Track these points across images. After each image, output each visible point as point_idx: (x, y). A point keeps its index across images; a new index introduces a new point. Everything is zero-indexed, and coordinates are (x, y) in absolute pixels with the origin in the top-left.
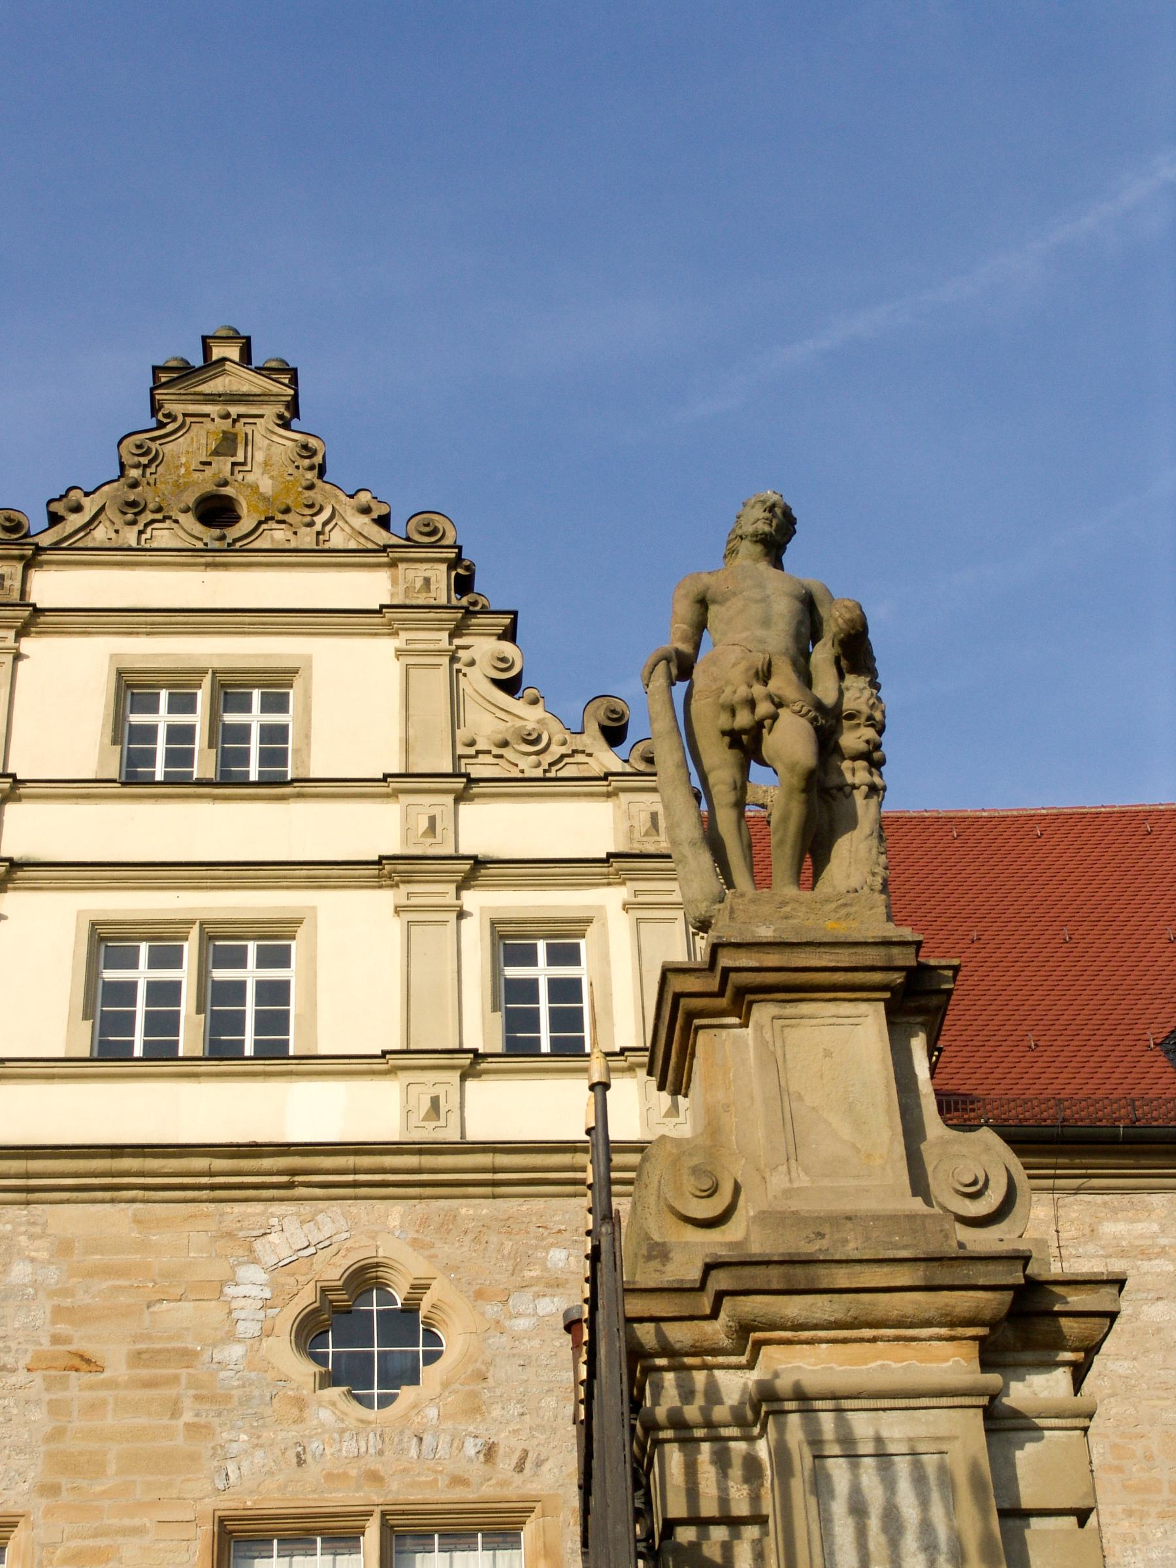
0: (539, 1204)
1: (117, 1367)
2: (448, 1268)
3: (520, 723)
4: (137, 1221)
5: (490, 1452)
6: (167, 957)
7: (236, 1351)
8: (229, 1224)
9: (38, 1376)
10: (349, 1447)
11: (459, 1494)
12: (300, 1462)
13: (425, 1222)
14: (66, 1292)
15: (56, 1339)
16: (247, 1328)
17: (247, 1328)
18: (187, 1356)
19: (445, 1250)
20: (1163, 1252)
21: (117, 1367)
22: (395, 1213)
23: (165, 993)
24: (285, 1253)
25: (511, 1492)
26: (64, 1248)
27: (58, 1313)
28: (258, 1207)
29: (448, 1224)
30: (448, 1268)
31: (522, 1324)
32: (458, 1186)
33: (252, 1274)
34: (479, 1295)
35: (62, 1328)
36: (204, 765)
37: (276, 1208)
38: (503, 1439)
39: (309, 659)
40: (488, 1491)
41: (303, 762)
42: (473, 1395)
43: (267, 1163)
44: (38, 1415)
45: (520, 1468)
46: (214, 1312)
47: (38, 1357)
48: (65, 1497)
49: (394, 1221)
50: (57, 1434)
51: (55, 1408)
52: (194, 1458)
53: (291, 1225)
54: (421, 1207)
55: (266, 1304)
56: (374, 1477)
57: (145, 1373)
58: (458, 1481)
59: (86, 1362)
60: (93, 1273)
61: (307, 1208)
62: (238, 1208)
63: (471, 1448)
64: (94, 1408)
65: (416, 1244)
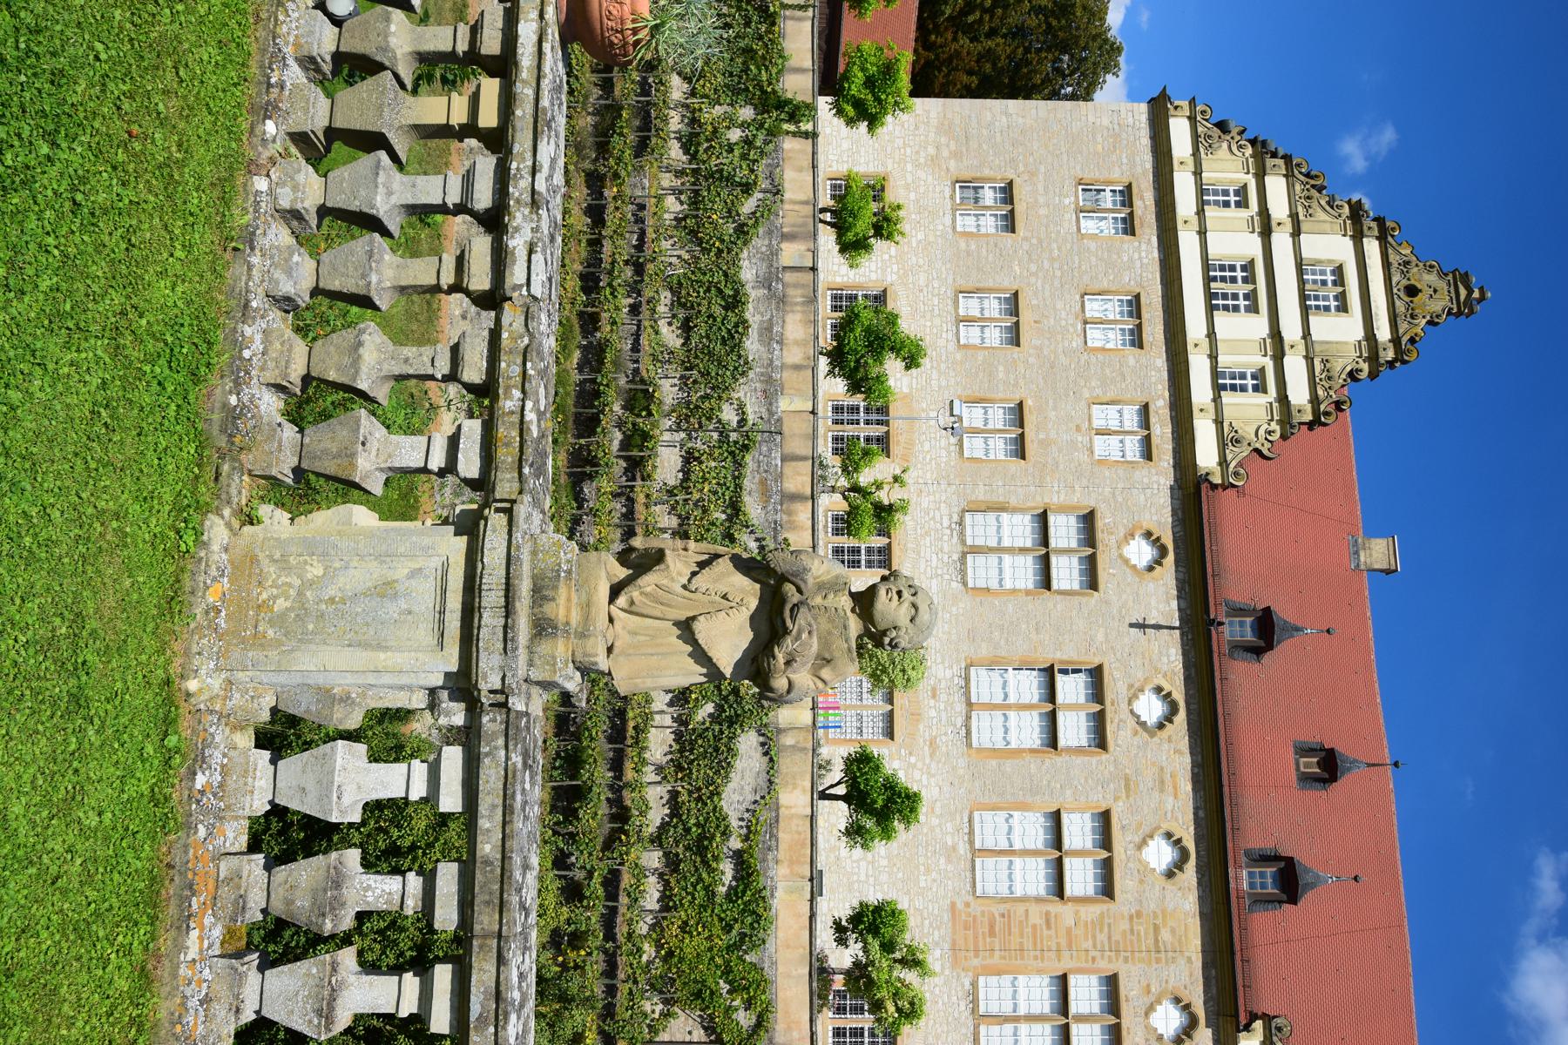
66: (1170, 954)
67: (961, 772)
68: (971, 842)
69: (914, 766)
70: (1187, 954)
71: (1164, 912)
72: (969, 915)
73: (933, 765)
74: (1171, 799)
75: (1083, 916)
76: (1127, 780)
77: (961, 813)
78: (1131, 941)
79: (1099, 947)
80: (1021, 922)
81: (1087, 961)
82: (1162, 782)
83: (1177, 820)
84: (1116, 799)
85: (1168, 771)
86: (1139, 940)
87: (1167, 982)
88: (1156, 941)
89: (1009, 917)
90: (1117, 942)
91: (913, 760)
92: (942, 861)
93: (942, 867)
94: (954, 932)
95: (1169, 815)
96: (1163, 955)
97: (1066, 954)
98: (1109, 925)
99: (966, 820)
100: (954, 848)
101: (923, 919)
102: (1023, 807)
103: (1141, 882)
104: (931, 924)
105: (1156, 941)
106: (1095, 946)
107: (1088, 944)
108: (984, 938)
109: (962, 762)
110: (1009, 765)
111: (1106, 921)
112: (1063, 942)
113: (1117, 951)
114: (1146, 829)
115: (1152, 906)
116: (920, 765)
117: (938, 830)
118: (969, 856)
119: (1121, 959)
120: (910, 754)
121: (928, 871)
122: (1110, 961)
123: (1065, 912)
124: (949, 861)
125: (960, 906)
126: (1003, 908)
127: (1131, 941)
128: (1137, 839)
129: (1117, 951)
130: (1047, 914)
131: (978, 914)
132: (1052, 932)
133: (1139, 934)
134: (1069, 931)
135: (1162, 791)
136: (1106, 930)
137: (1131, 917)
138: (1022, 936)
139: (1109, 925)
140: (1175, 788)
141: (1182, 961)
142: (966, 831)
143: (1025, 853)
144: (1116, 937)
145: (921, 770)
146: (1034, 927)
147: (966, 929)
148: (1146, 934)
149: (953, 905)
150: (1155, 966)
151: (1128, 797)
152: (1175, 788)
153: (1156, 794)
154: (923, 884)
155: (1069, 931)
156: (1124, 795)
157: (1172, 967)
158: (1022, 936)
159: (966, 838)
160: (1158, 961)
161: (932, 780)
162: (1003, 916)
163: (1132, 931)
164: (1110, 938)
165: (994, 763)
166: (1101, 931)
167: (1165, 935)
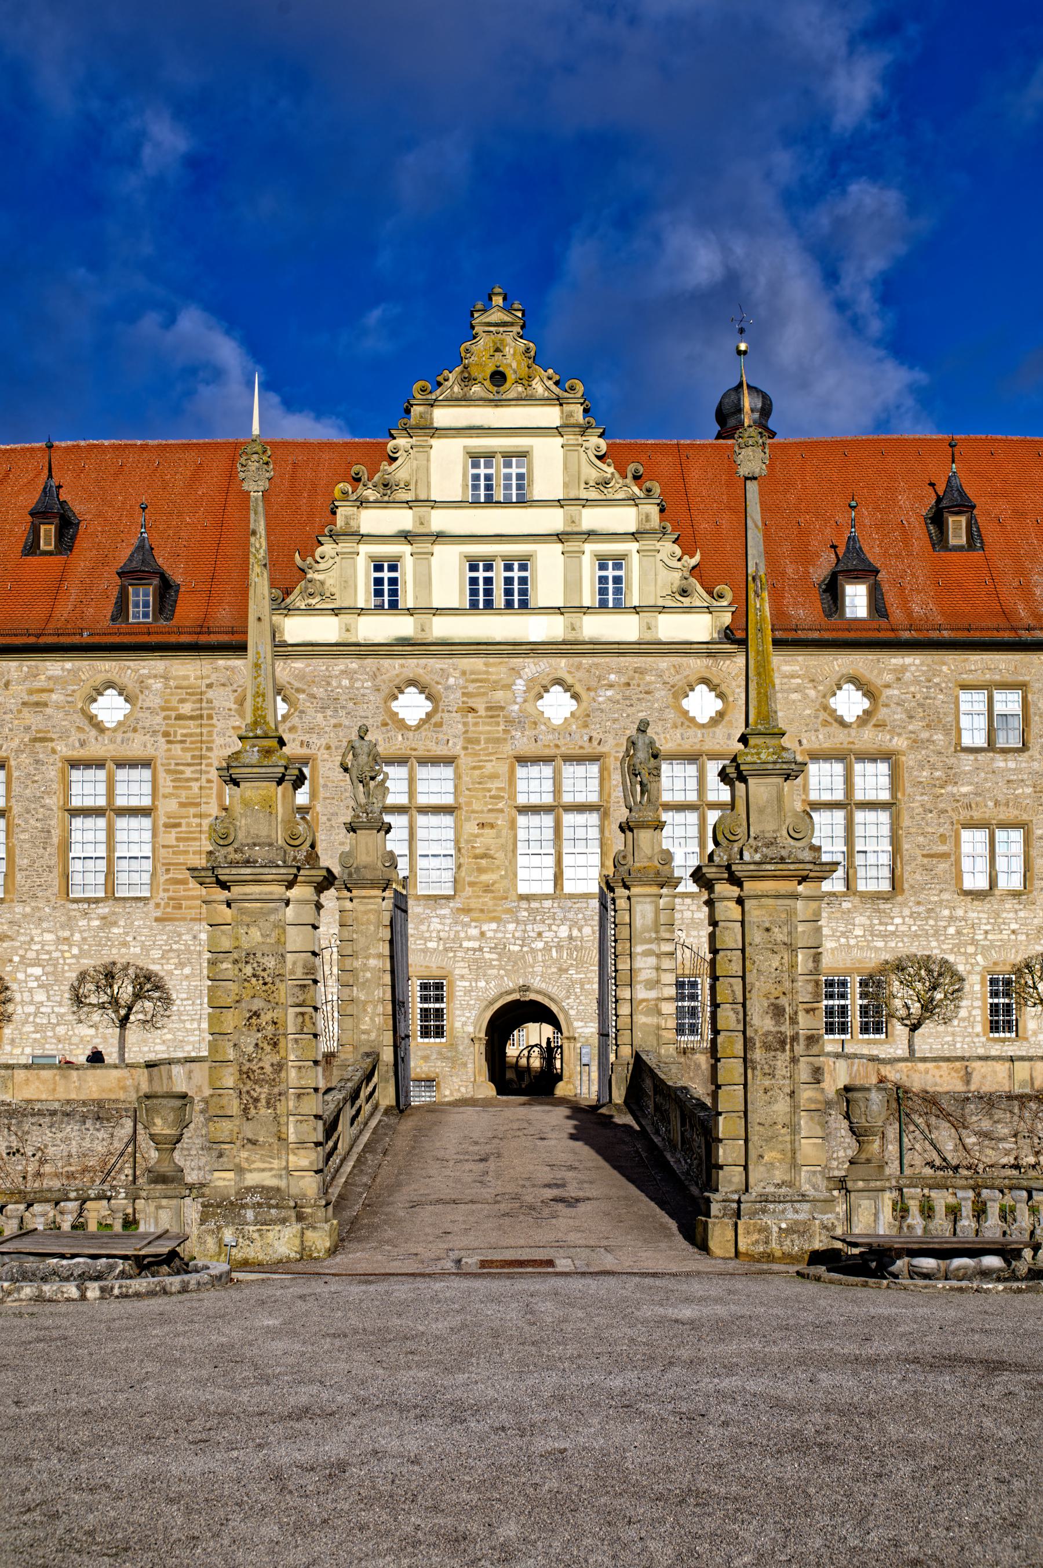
0: (607, 660)
1: (482, 712)
2: (580, 681)
3: (606, 475)
4: (486, 664)
5: (591, 739)
6: (488, 568)
7: (516, 707)
8: (512, 666)
9: (459, 714)
10: (551, 737)
11: (581, 751)
12: (536, 741)
13: (572, 665)
14: (466, 688)
15: (463, 703)
16: (519, 700)
17: (519, 700)
18: (502, 708)
19: (579, 674)
20: (798, 677)
21: (482, 712)
22: (563, 662)
23: (488, 581)
24: (530, 674)
25: (596, 751)
26: (464, 673)
27: (464, 694)
28: (521, 660)
29: (579, 667)
30: (580, 681)
31: (601, 699)
32: (583, 654)
33: (519, 682)
34: (588, 689)
35: (465, 699)
36: (499, 495)
37: (527, 660)
38: (594, 734)
39: (532, 447)
40: (590, 750)
41: (531, 492)
42: (586, 721)
43: (524, 647)
44: (460, 726)
45: (599, 744)
46: (509, 694)
47: (459, 708)
48: (470, 751)
49: (563, 665)
50: (466, 732)
51: (465, 724)
52: (505, 739)
53: (532, 666)
54: (571, 660)
55: (525, 692)
56: (557, 746)
57: (490, 713)
58: (581, 747)
59: (472, 710)
60: (474, 681)
61: (536, 660)
62: (515, 660)
63: (586, 738)
64: (476, 724)
65: (569, 672)
66: (204, 705)
67: (28, 910)
68: (97, 901)
69: (22, 957)
70: (204, 689)
71: (163, 709)
72: (167, 905)
73: (22, 938)
74: (54, 697)
75: (170, 790)
76: (35, 740)
77: (70, 910)
78: (192, 743)
79: (197, 776)
80: (174, 853)
81: (211, 788)
82: (37, 704)
83: (74, 691)
84: (54, 751)
85: (26, 698)
86: (191, 735)
87: (230, 710)
88: (191, 718)
89: (169, 864)
90: (193, 757)
91: (16, 959)
92: (115, 930)
93: (121, 931)
94: (184, 919)
95: (70, 699)
96: (205, 712)
97: (204, 808)
98: (177, 764)
99: (75, 906)
100: (104, 918)
101: (171, 950)
102: (66, 845)
103: (135, 730)
104: (176, 943)
105: (191, 718)
106: (197, 780)
107: (195, 785)
108: (189, 890)
109: (19, 909)
110: (23, 862)
111: (172, 767)
112: (192, 811)
113: (201, 757)
114: (84, 723)
115: (158, 719)
116: (21, 952)
117: (86, 935)
118: (111, 902)
119: (209, 754)
120: (11, 961)
121: (125, 944)
122: (209, 765)
123: (168, 807)
124: (115, 924)
125: (159, 914)
126: (161, 869)
127: (192, 743)
128: (94, 733)
129: (201, 757)
130: (166, 826)
131: (166, 895)
132: (183, 821)
133: (185, 735)
134: (182, 805)
135: (46, 705)
136: (181, 768)
137: (169, 742)
138: (186, 852)
139: (177, 764)
140: (43, 691)
141: (210, 694)
142: (86, 906)
143: (111, 843)
144: (188, 757)
145: (26, 950)
146: (178, 839)
147: (180, 908)
148: (185, 728)
149: (157, 920)
150: (214, 721)
151: (52, 740)
152: (43, 691)
153: (49, 711)
154: (138, 950)
155: (182, 805)
156: (50, 744)
157: (216, 703)
158: (186, 852)
159: (94, 906)
160: (210, 717)
161: (36, 939)
162: (168, 870)
163: (182, 742)
164: (189, 765)
165: (19, 876)
166: (182, 772)
167: (186, 709)
